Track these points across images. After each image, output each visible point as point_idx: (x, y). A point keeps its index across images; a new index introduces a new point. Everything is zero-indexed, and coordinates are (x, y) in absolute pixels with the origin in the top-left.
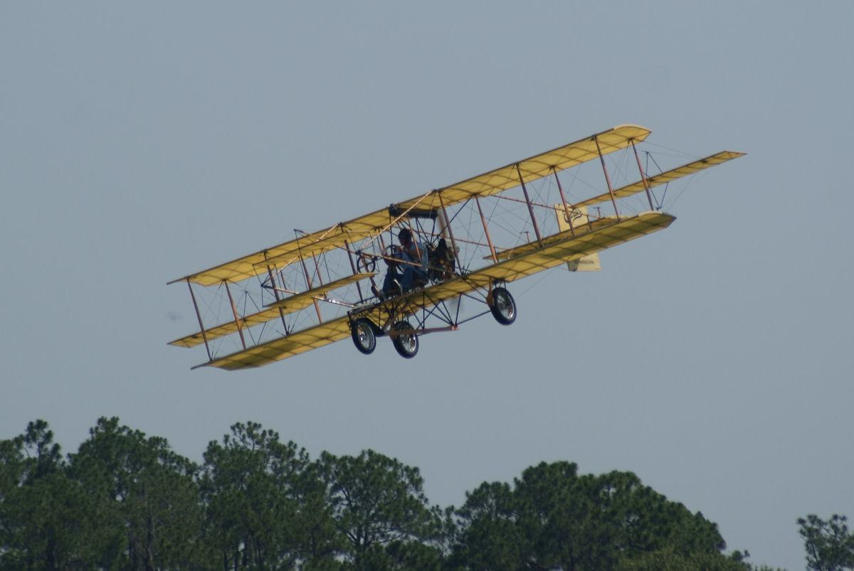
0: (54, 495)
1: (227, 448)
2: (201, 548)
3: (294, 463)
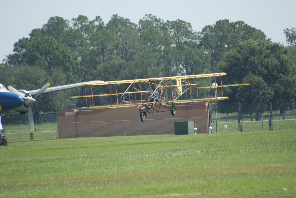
3: (160, 23)
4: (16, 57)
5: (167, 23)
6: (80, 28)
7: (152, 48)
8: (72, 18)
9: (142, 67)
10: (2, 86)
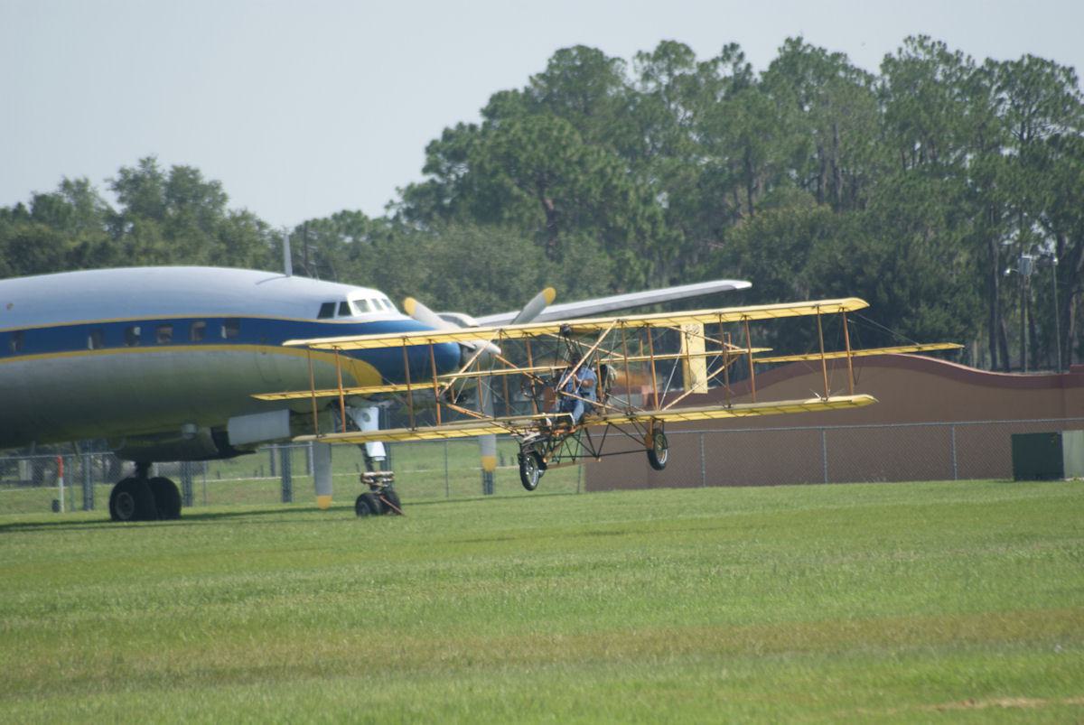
0: (748, 108)
2: (880, 149)
3: (962, 69)
4: (433, 195)
6: (663, 89)
7: (930, 161)
8: (634, 53)
9: (893, 230)
10: (384, 301)
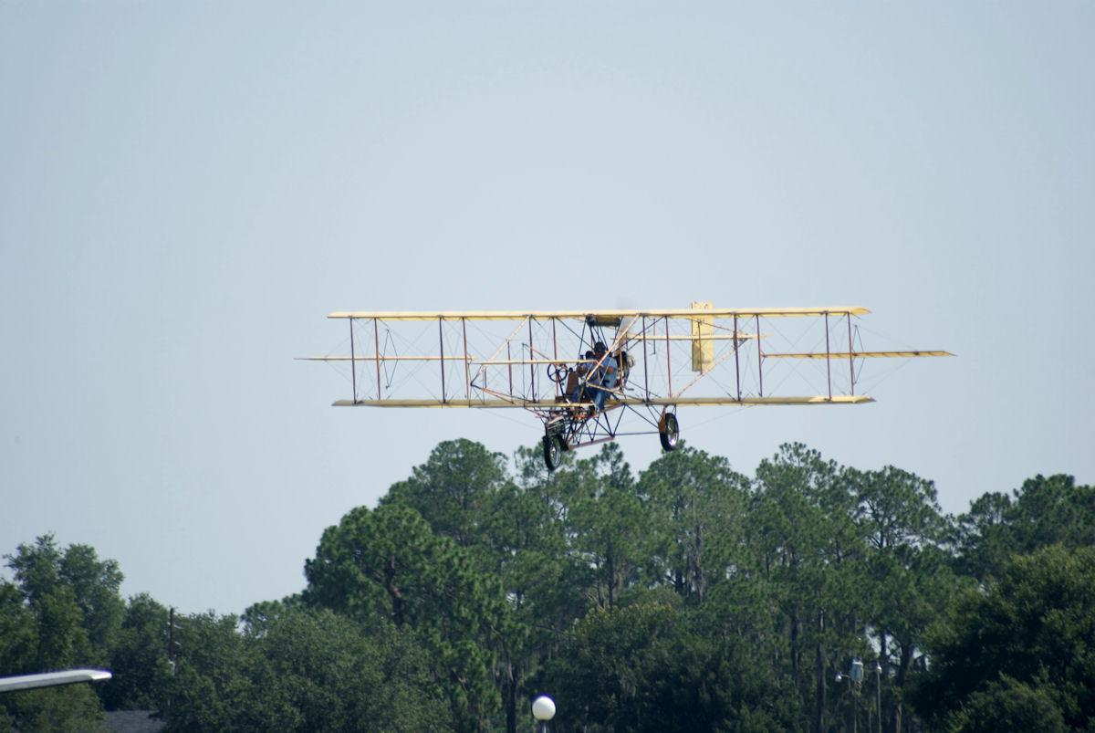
1: (777, 465)
5: (850, 477)
